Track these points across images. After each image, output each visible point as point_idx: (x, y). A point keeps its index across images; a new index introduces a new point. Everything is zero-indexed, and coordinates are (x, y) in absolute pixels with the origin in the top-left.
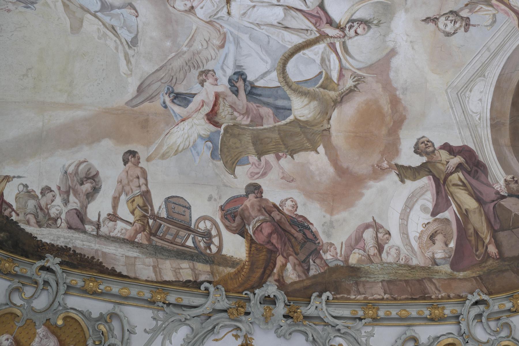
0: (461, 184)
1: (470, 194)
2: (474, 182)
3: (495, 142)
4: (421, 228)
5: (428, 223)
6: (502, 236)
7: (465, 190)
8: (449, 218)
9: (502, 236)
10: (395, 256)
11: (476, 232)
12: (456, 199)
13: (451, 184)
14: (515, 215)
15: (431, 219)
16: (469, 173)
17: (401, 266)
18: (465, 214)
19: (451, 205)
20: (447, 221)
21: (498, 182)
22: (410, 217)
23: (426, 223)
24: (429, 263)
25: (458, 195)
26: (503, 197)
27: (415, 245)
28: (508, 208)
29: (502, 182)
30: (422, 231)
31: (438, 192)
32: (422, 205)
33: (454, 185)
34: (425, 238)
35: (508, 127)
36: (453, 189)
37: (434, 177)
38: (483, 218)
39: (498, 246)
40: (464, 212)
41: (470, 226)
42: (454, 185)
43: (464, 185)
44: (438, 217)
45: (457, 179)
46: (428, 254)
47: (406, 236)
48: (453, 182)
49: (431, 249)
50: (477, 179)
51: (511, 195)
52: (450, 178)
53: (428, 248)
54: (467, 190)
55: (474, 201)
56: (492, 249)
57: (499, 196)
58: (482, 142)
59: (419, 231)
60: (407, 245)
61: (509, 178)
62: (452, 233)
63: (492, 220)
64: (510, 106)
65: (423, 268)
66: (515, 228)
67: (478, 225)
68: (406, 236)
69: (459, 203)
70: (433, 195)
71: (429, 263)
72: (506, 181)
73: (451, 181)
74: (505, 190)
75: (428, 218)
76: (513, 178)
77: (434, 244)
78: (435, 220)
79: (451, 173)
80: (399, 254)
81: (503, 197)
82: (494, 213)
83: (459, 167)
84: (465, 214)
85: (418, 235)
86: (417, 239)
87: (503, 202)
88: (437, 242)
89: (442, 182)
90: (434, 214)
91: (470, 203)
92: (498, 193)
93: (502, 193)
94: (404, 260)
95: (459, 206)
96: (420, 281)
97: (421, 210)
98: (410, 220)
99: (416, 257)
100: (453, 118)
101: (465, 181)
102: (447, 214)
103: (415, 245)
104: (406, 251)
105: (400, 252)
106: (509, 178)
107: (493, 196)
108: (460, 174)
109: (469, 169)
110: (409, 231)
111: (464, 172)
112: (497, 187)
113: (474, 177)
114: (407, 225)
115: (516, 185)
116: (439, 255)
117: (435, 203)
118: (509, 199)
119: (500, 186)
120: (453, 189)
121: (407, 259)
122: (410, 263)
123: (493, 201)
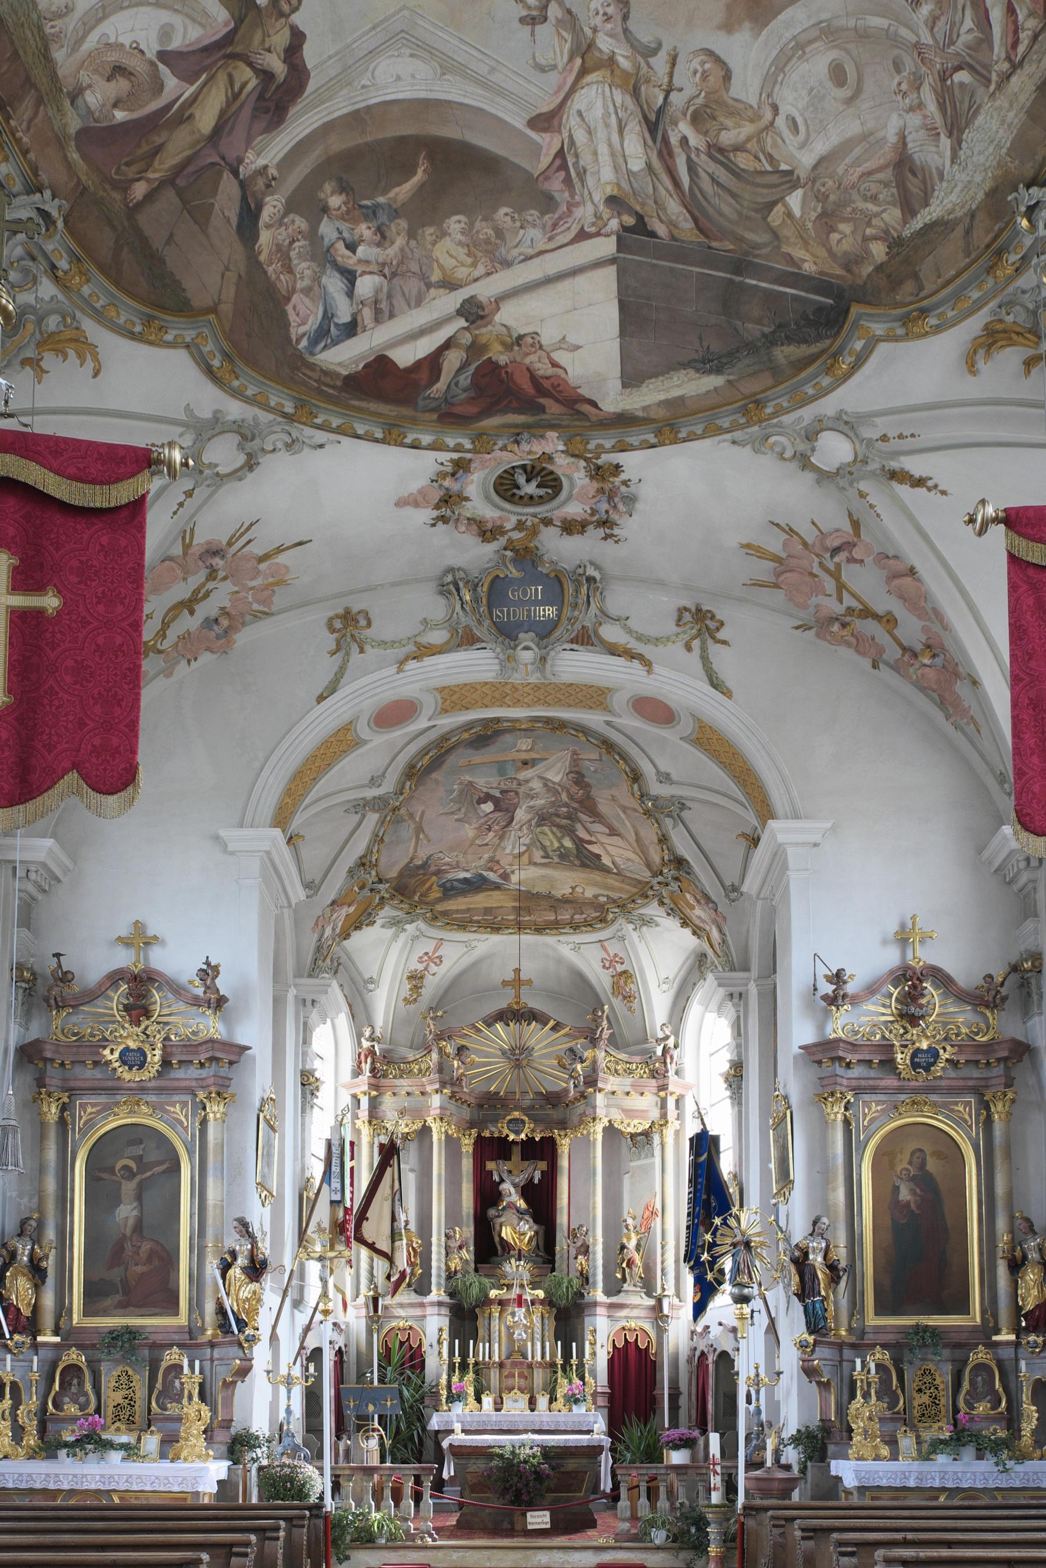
0: (236, 89)
1: (222, 113)
2: (246, 113)
3: (328, 128)
4: (126, 40)
5: (142, 52)
6: (170, 195)
7: (227, 102)
8: (166, 90)
9: (170, 195)
10: (54, 8)
11: (158, 149)
12: (205, 90)
13: (230, 69)
14: (213, 205)
15: (151, 55)
16: (261, 98)
17: (40, 29)
18: (183, 117)
19: (192, 84)
20: (158, 87)
21: (258, 155)
22: (142, 9)
23: (142, 47)
24: (68, 87)
25: (214, 91)
26: (235, 173)
27: (92, 41)
28: (220, 188)
29: (261, 162)
30: (122, 45)
31: (207, 50)
32: (171, 26)
33: (231, 78)
34: (112, 57)
35: (360, 141)
36: (222, 78)
37: (234, 32)
38: (188, 153)
39: (150, 197)
40: (187, 114)
41: (165, 135)
42: (231, 78)
43: (236, 96)
44: (161, 66)
45: (244, 79)
46: (85, 78)
47: (100, 15)
48: (234, 73)
49: (96, 77)
50: (254, 117)
51: (242, 184)
52: (242, 65)
53: (96, 71)
54: (228, 104)
55: (213, 123)
56: (140, 190)
57: (235, 164)
58: (323, 103)
59: (121, 40)
60: (84, 24)
61: (272, 171)
62: (141, 107)
63: (191, 169)
64: (398, 134)
65: (54, 77)
66: (189, 213)
67: (171, 147)
68: (100, 15)
69: (200, 98)
70: (198, 40)
71: (68, 87)
72: (266, 167)
73: (235, 68)
74: (249, 172)
75: (151, 47)
76: (274, 179)
77: (108, 80)
78: (152, 64)
79: (250, 65)
80: (59, 15)
81: (235, 173)
82: (203, 168)
83: (266, 76)
84: (183, 117)
85: (112, 40)
86: (104, 40)
87: (227, 176)
88: (113, 83)
89: (229, 51)
90: (163, 56)
91: (206, 120)
92: (240, 160)
93: (241, 169)
94: (53, 30)
95: (194, 100)
96: (28, 82)
97: (162, 27)
98: (133, 11)
99: (69, 56)
100: (355, 35)
101: (243, 96)
102: (171, 82)
103: (92, 41)
104: (71, 28)
105: (66, 14)
106: (272, 171)
107: (231, 155)
108: (253, 82)
109: (267, 96)
110: (113, 19)
111: (260, 88)
112: (250, 155)
113: (255, 109)
114: (122, 8)
115: (263, 188)
116: (92, 99)
117: (185, 50)
118: (235, 184)
119: (253, 162)
120: (222, 78)
121: (57, 36)
122: (53, 47)
123: (223, 159)
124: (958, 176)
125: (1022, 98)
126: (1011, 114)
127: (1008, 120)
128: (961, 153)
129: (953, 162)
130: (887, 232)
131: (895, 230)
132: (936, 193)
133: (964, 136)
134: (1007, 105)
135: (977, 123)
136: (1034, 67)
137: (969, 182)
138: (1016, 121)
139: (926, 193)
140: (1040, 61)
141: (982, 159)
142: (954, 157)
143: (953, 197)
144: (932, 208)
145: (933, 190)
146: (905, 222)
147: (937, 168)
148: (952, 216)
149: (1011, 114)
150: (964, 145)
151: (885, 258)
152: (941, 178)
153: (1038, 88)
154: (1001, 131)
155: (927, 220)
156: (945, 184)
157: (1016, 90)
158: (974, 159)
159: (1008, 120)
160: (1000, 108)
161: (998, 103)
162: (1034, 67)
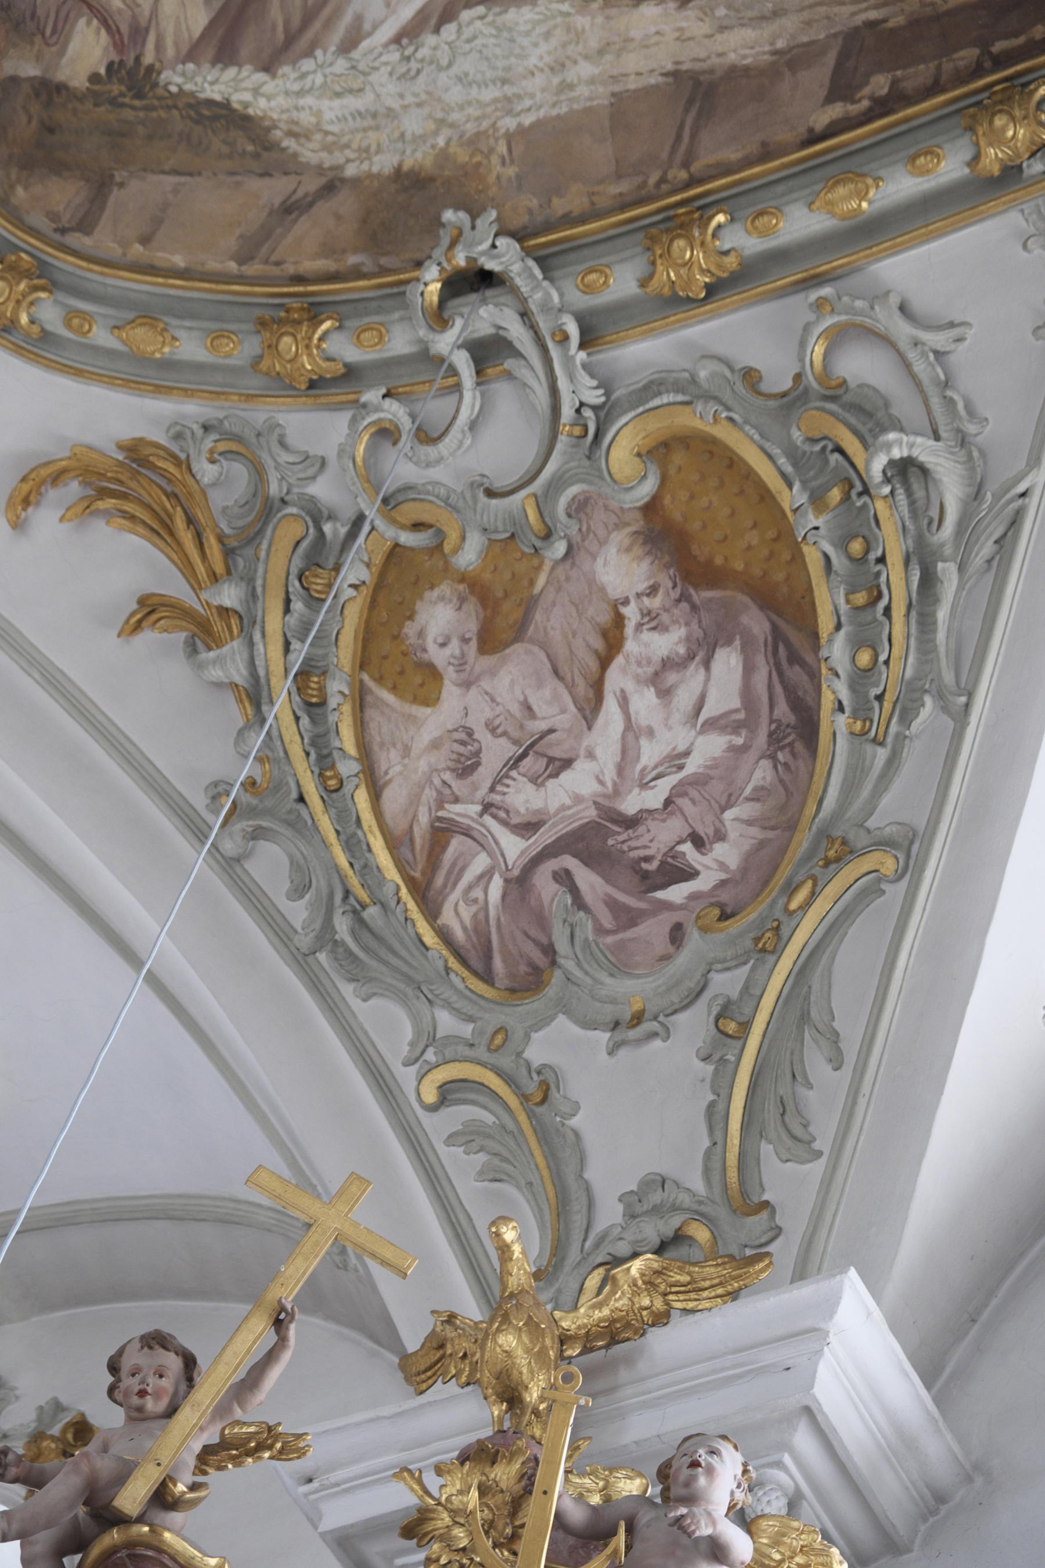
124: (380, 77)
125: (632, 62)
126: (586, 69)
127: (571, 75)
128: (430, 40)
129: (397, 40)
130: (139, 33)
131: (159, 47)
132: (307, 65)
133: (466, 15)
134: (594, 44)
135: (512, 14)
136: (705, 28)
137: (390, 113)
138: (582, 91)
139: (290, 40)
140: (723, 29)
141: (455, 94)
142: (409, 34)
143: (331, 110)
144: (270, 86)
145: (309, 53)
146: (192, 55)
147: (359, 19)
148: (288, 143)
149: (586, 69)
150: (449, 31)
151: (79, 81)
152: (348, 46)
153: (675, 74)
154: (539, 80)
155: (238, 99)
156: (341, 65)
157: (636, 34)
158: (443, 78)
159: (571, 75)
160: (579, 36)
161: (582, 21)
162: (705, 28)
